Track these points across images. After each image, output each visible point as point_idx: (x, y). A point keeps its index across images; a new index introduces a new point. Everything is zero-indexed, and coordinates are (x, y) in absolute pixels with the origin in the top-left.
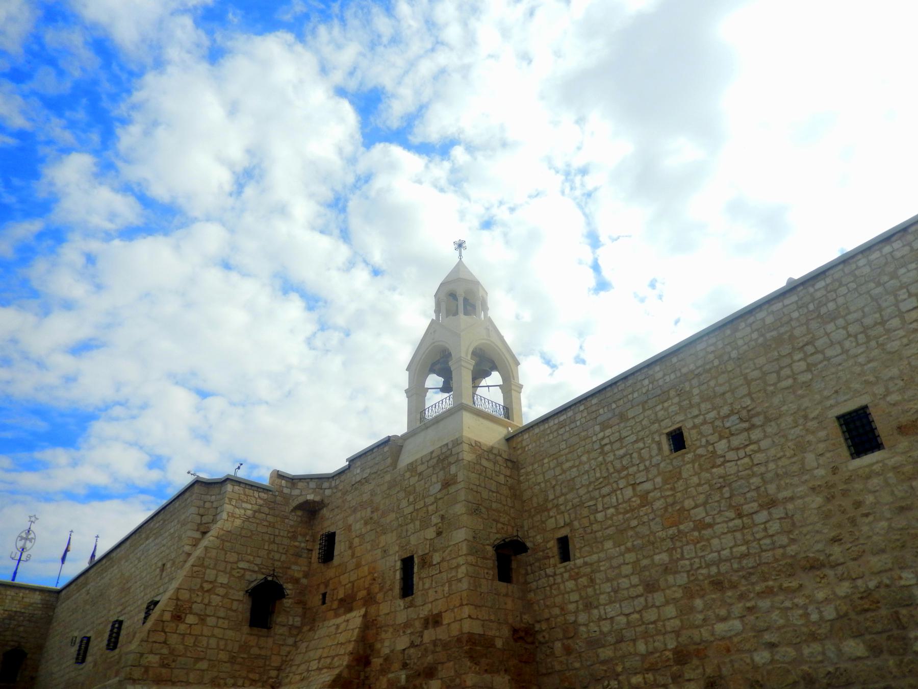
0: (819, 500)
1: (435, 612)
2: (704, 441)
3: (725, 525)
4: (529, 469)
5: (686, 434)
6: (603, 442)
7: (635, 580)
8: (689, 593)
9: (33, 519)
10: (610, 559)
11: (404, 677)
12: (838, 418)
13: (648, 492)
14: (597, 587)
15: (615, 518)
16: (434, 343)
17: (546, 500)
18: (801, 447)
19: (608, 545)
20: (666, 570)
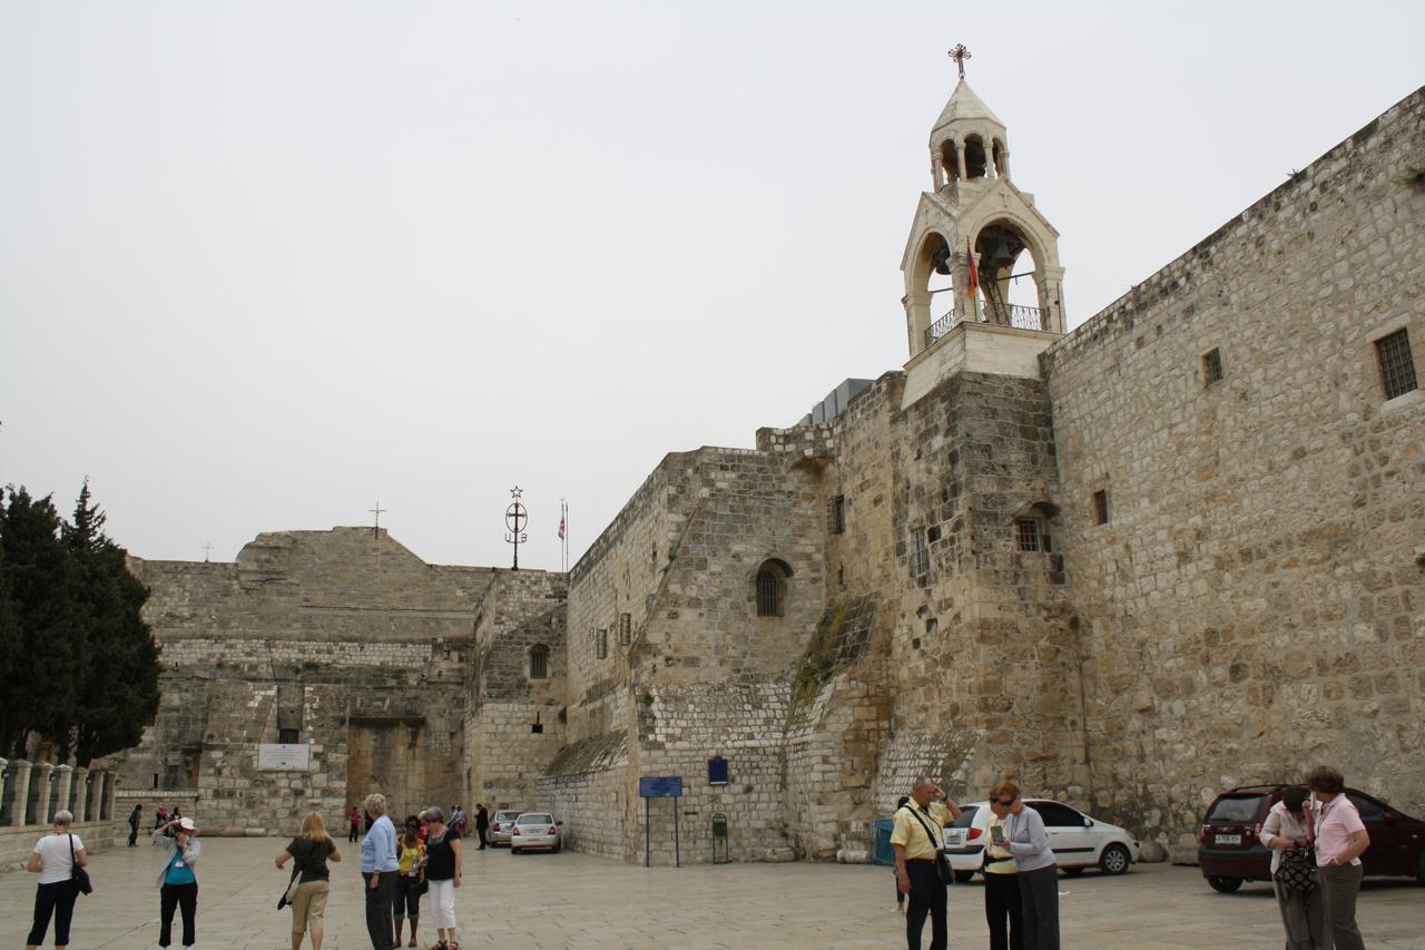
0: (1348, 452)
1: (947, 596)
2: (1240, 367)
3: (1256, 482)
4: (1063, 400)
5: (1222, 358)
6: (1138, 367)
7: (1170, 548)
8: (1222, 564)
9: (516, 492)
10: (1146, 519)
11: (923, 666)
12: (1378, 343)
13: (1182, 434)
14: (1133, 556)
15: (1151, 469)
16: (928, 229)
17: (1081, 443)
18: (1338, 381)
19: (1145, 502)
20: (1200, 535)
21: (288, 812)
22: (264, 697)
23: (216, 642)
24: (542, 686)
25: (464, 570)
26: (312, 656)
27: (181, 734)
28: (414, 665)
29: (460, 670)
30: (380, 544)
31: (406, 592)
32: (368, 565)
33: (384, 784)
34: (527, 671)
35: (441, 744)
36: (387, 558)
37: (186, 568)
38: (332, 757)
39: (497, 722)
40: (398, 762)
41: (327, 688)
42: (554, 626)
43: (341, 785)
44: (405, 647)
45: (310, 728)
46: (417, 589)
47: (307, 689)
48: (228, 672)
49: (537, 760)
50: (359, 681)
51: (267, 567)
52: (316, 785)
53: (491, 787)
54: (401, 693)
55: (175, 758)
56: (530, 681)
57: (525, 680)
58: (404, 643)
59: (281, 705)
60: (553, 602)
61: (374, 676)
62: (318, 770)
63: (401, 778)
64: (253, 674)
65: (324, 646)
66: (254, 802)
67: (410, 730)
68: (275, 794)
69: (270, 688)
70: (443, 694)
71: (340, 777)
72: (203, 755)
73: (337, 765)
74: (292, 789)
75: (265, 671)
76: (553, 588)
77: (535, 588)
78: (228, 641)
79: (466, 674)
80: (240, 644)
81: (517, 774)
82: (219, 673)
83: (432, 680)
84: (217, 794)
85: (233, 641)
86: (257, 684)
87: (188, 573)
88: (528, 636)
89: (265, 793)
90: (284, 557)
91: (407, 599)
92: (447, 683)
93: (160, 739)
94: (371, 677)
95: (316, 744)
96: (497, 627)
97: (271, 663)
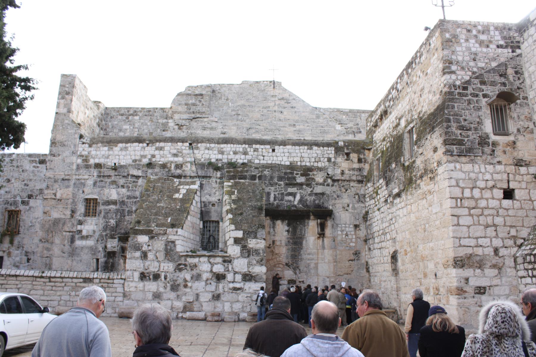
21: (210, 296)
22: (188, 190)
23: (148, 144)
24: (508, 145)
25: (340, 111)
26: (230, 157)
27: (117, 225)
28: (320, 165)
29: (360, 170)
30: (277, 92)
31: (298, 127)
32: (269, 107)
33: (298, 273)
34: (488, 127)
35: (347, 235)
36: (282, 102)
37: (135, 111)
38: (252, 243)
39: (461, 184)
40: (309, 251)
41: (244, 183)
42: (511, 78)
43: (260, 270)
44: (311, 149)
45: (230, 216)
46: (307, 125)
47: (225, 184)
48: (157, 170)
49: (513, 232)
50: (272, 178)
51: (193, 109)
52: (237, 270)
53: (462, 266)
54: (309, 190)
55: (113, 244)
56: (494, 138)
57: (488, 137)
58: (310, 145)
59: (204, 199)
60: (506, 53)
61: (286, 173)
62: (239, 255)
63: (312, 265)
64: (179, 171)
65: (240, 148)
66: (179, 285)
67: (319, 220)
68: (198, 277)
69: (193, 183)
70: (346, 190)
71: (260, 262)
72: (130, 239)
73: (257, 252)
74: (215, 273)
75: (189, 169)
76: (504, 38)
77: (483, 37)
78: (157, 144)
79: (365, 173)
80: (168, 147)
81: (492, 250)
82: (150, 171)
83: (338, 178)
84: (143, 276)
85: (162, 144)
86: (182, 180)
87: (136, 115)
88: (483, 87)
89: (188, 277)
90: (206, 101)
91: (299, 131)
92: (349, 181)
93: (101, 227)
94: (283, 175)
95: (236, 229)
96: (447, 76)
97: (195, 163)
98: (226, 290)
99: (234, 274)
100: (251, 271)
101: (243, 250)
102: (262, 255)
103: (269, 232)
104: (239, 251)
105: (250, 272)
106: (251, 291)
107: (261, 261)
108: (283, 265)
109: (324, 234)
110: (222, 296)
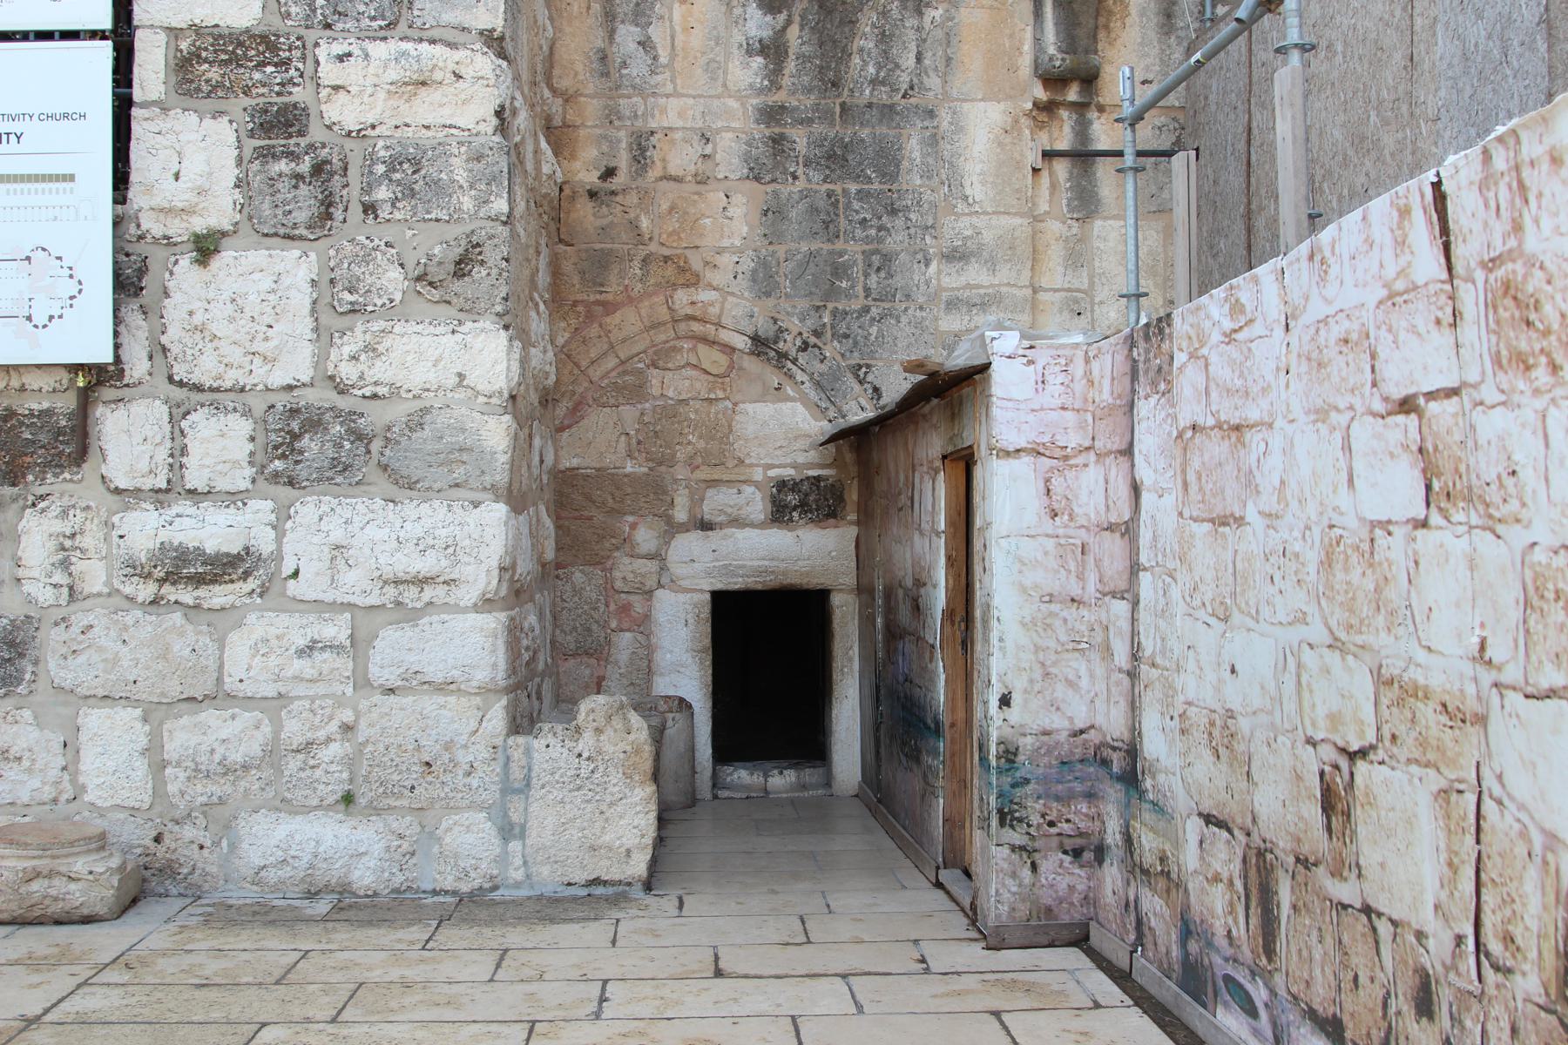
40: (957, 228)
52: (205, 370)
98: (94, 575)
99: (178, 415)
100: (348, 372)
101: (266, 155)
102: (467, 203)
103: (604, 58)
104: (231, 173)
105: (342, 390)
106: (355, 584)
107: (461, 267)
108: (729, 349)
109: (1089, 79)
110: (53, 639)
